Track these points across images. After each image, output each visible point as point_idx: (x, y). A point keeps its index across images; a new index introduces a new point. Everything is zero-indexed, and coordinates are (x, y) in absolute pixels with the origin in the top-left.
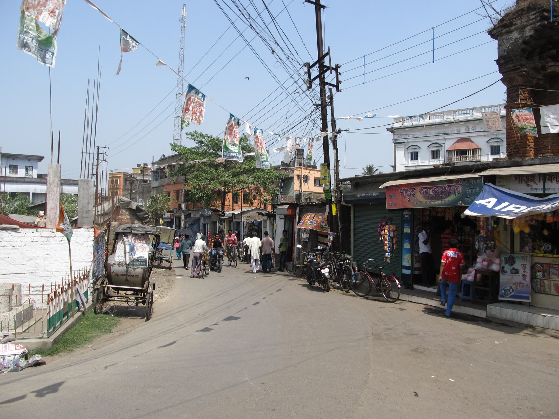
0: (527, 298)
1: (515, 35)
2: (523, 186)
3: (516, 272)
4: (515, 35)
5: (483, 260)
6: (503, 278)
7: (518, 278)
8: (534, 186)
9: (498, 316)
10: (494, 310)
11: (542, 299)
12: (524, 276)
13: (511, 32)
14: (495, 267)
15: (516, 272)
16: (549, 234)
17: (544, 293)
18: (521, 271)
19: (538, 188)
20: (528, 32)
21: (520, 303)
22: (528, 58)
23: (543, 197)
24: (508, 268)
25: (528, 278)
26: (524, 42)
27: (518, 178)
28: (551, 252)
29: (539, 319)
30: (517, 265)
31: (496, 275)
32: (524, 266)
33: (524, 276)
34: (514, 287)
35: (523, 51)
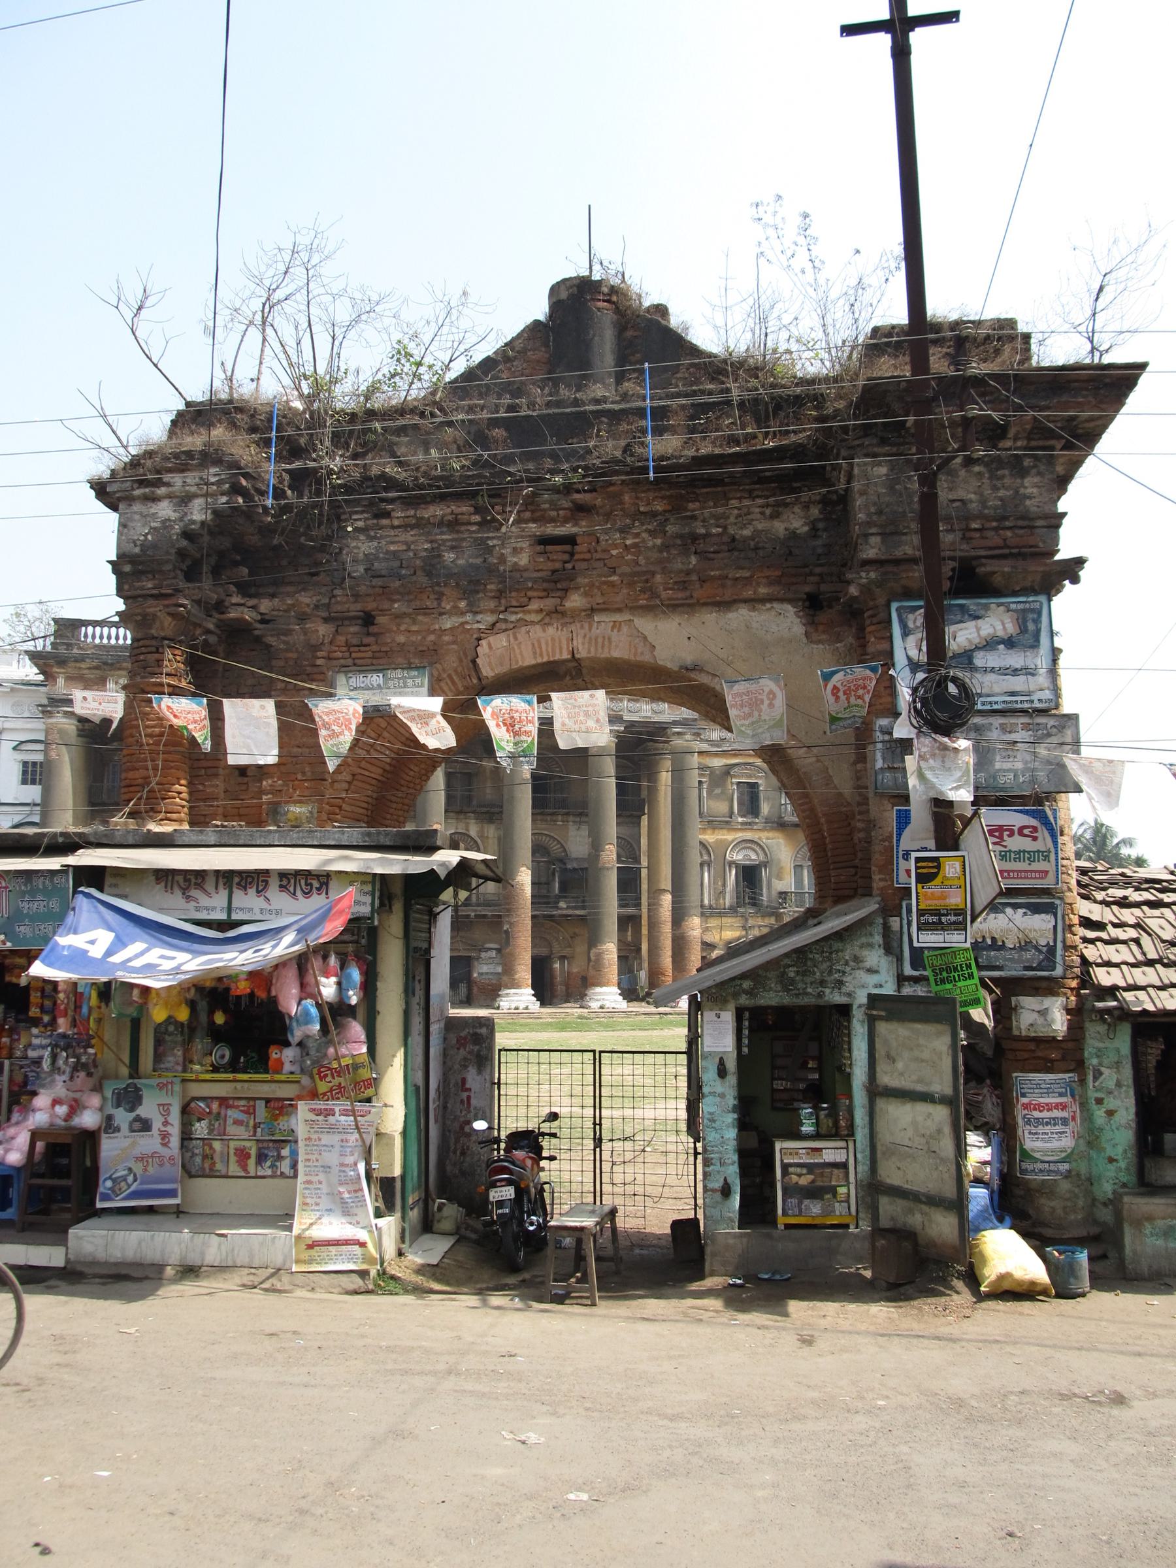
0: (172, 1193)
1: (165, 510)
2: (176, 899)
3: (144, 1125)
4: (165, 510)
5: (56, 1102)
6: (109, 1147)
7: (149, 1143)
8: (204, 901)
9: (101, 1255)
10: (90, 1240)
11: (211, 1192)
12: (165, 1136)
13: (155, 499)
14: (88, 1119)
15: (144, 1125)
16: (226, 1023)
17: (212, 1174)
18: (157, 1124)
19: (214, 905)
20: (198, 513)
21: (151, 1210)
22: (192, 574)
23: (226, 929)
24: (122, 1117)
25: (175, 1141)
26: (187, 534)
27: (165, 876)
28: (233, 1067)
29: (212, 1248)
30: (148, 1109)
31: (90, 1138)
32: (165, 1109)
33: (165, 1136)
34: (138, 1168)
35: (182, 554)
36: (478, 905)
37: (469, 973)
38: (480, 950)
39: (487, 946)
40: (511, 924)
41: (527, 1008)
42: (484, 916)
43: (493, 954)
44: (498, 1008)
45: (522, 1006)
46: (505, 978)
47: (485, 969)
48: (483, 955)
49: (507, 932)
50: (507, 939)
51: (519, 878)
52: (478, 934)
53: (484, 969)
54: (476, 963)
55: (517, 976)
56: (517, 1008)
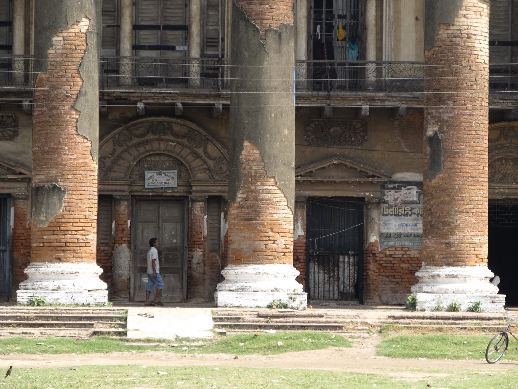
36: (379, 86)
37: (361, 234)
38: (383, 186)
39: (399, 176)
40: (442, 123)
41: (474, 309)
42: (392, 112)
43: (413, 193)
44: (413, 306)
45: (465, 303)
46: (430, 243)
47: (393, 225)
48: (390, 196)
49: (434, 140)
50: (436, 155)
51: (461, 22)
52: (381, 149)
53: (391, 226)
54: (375, 214)
55: (453, 239)
56: (453, 308)
